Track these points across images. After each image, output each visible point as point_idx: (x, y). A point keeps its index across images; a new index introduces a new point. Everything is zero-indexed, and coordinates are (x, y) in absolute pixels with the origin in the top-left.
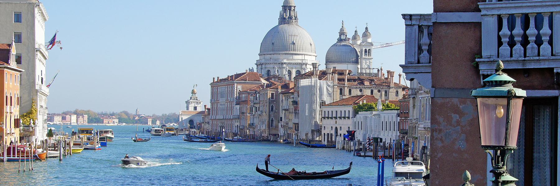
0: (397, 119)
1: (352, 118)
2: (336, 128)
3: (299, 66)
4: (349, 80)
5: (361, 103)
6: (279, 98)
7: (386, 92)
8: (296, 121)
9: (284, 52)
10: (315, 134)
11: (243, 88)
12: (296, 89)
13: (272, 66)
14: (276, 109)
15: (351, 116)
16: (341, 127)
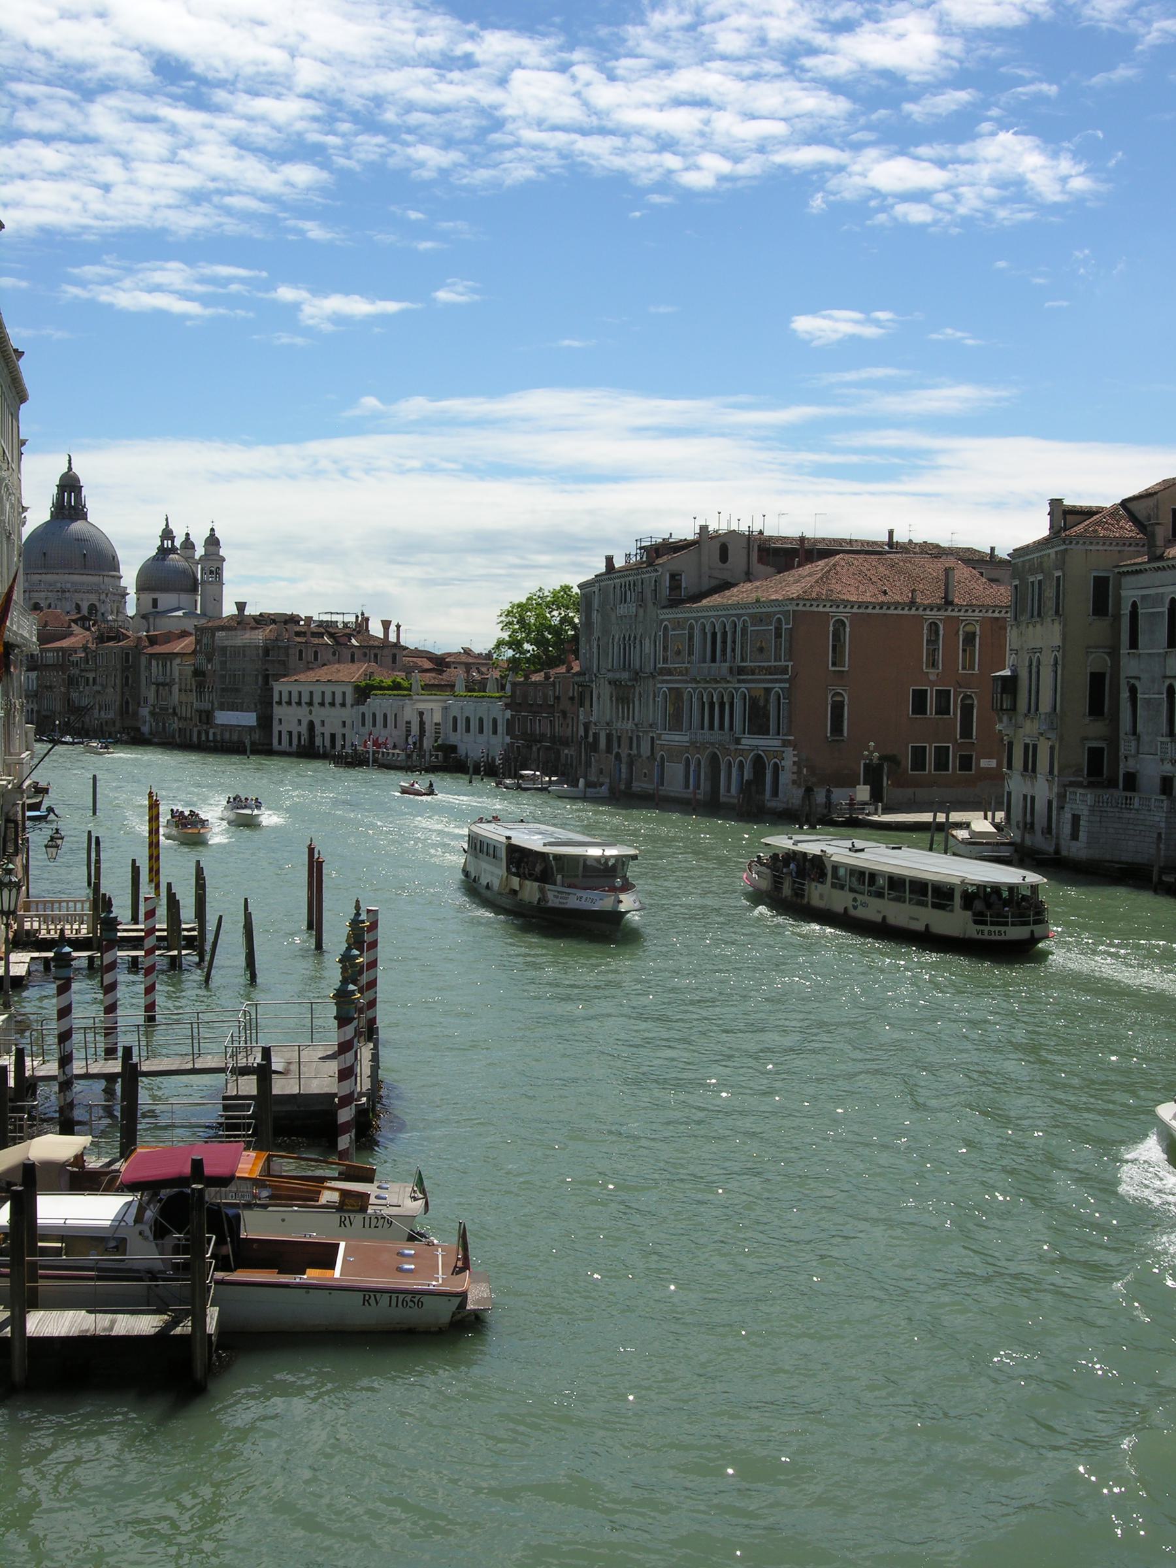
0: (504, 715)
1: (352, 706)
2: (311, 725)
7: (376, 656)
8: (207, 706)
12: (201, 648)
13: (43, 595)
15: (349, 701)
16: (323, 722)
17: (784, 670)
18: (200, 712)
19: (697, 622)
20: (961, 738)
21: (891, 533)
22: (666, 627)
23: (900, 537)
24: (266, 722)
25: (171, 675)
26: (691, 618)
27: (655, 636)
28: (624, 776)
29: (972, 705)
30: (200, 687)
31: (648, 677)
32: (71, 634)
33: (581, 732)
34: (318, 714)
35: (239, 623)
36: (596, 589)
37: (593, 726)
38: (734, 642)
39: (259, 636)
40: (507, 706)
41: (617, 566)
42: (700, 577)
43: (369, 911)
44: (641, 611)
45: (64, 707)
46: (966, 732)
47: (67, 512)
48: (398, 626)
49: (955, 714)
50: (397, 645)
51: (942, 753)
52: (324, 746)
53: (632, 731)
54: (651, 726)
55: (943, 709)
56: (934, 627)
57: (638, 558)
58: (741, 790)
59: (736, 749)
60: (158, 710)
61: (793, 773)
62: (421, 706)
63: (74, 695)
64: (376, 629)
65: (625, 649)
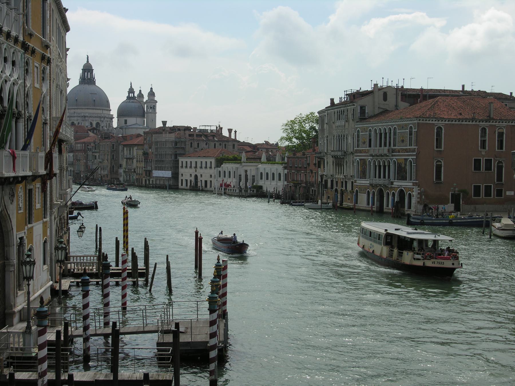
0: (284, 172)
1: (215, 168)
2: (196, 176)
3: (98, 119)
7: (225, 145)
8: (149, 168)
9: (86, 107)
10: (172, 180)
12: (146, 142)
13: (75, 118)
15: (213, 166)
16: (201, 175)
17: (414, 150)
18: (146, 171)
19: (373, 129)
20: (497, 181)
21: (463, 86)
22: (358, 130)
23: (468, 88)
24: (176, 176)
25: (133, 154)
26: (370, 127)
27: (353, 135)
28: (339, 200)
29: (502, 166)
31: (350, 154)
32: (88, 136)
33: (320, 180)
34: (199, 172)
35: (164, 130)
36: (326, 114)
37: (325, 177)
38: (390, 138)
39: (172, 137)
40: (285, 168)
41: (335, 103)
42: (374, 108)
43: (223, 261)
44: (347, 124)
45: (85, 169)
46: (500, 178)
47: (86, 81)
48: (235, 132)
49: (494, 170)
50: (235, 140)
51: (488, 189)
52: (202, 186)
53: (343, 179)
54: (351, 176)
55: (488, 168)
56: (484, 130)
57: (345, 99)
58: (393, 206)
59: (391, 187)
60: (127, 170)
61: (418, 198)
62: (246, 168)
63: (90, 163)
64: (225, 133)
65: (339, 141)
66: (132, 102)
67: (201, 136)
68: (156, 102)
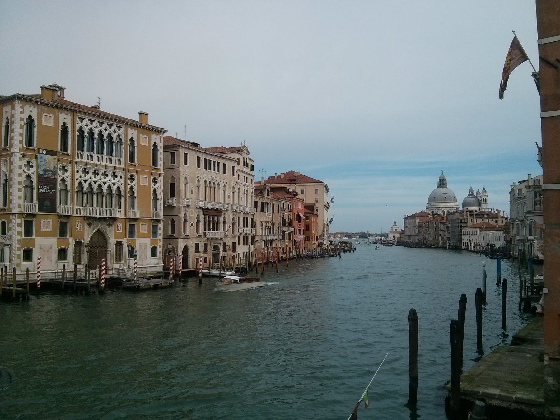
0: (503, 235)
4: (476, 215)
5: (483, 226)
6: (439, 225)
7: (496, 221)
11: (420, 220)
13: (434, 209)
14: (437, 230)
18: (448, 238)
30: (448, 231)
48: (504, 212)
66: (472, 197)
67: (479, 215)
68: (487, 196)
